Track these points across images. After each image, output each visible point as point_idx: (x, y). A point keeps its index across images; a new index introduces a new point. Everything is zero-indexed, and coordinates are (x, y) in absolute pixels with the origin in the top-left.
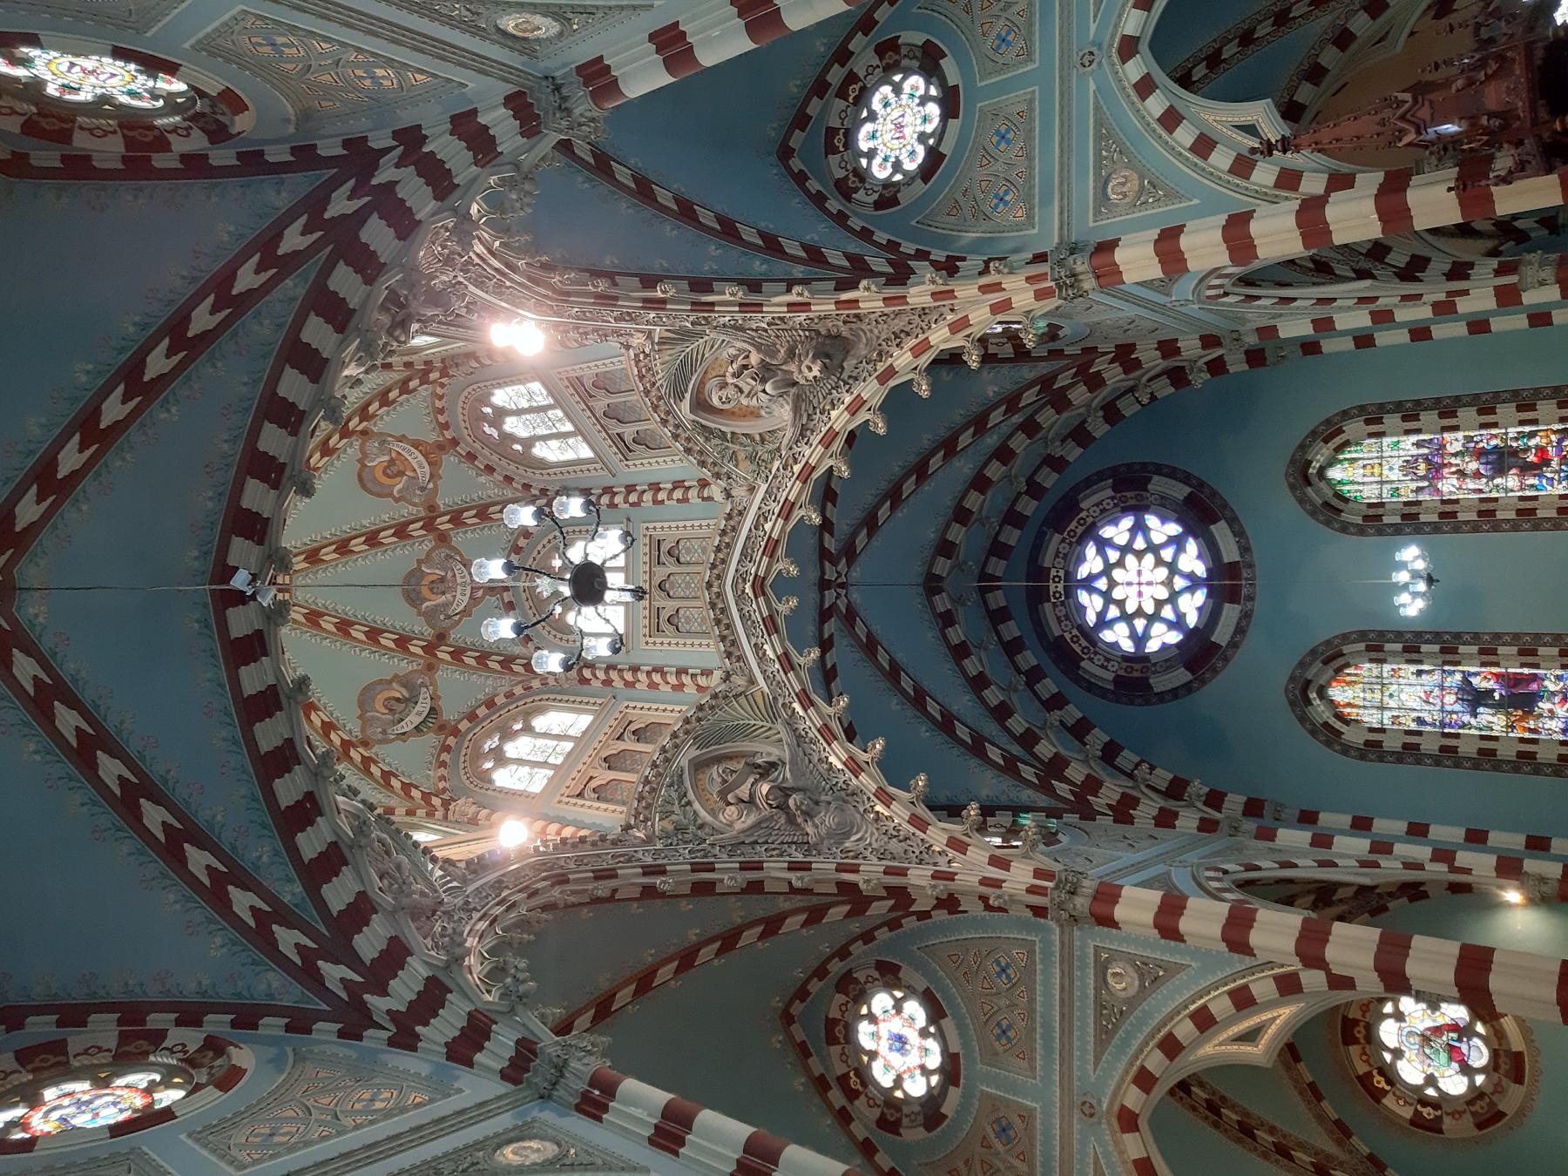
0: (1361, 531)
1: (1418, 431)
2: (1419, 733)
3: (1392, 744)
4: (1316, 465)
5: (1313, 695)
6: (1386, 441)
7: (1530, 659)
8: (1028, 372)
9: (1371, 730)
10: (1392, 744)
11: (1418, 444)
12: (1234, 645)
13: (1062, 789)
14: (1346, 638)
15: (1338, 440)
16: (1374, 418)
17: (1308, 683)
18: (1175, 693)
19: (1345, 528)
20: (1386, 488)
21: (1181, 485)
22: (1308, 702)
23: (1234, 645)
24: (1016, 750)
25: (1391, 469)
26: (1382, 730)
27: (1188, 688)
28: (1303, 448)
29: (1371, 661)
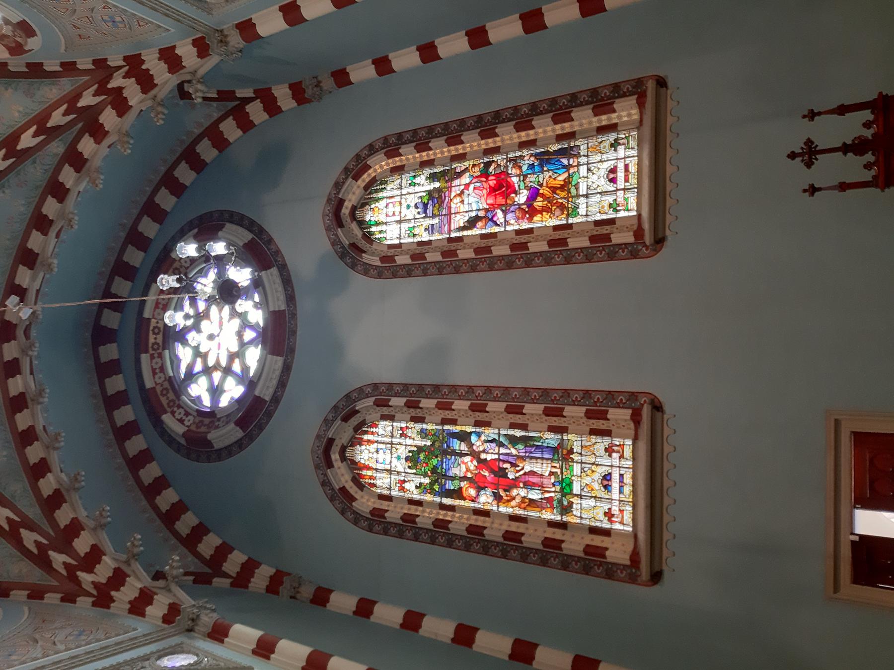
0: (380, 274)
1: (430, 163)
2: (419, 503)
3: (394, 514)
4: (348, 205)
5: (335, 457)
6: (406, 176)
7: (518, 419)
8: (51, 92)
9: (381, 497)
10: (394, 514)
11: (433, 177)
12: (276, 399)
13: (58, 559)
14: (361, 392)
15: (366, 177)
16: (391, 147)
17: (331, 441)
18: (230, 451)
19: (367, 270)
20: (405, 226)
21: (240, 230)
22: (330, 465)
23: (276, 399)
24: (34, 512)
25: (408, 207)
26: (389, 498)
27: (240, 445)
28: (338, 185)
29: (384, 417)
